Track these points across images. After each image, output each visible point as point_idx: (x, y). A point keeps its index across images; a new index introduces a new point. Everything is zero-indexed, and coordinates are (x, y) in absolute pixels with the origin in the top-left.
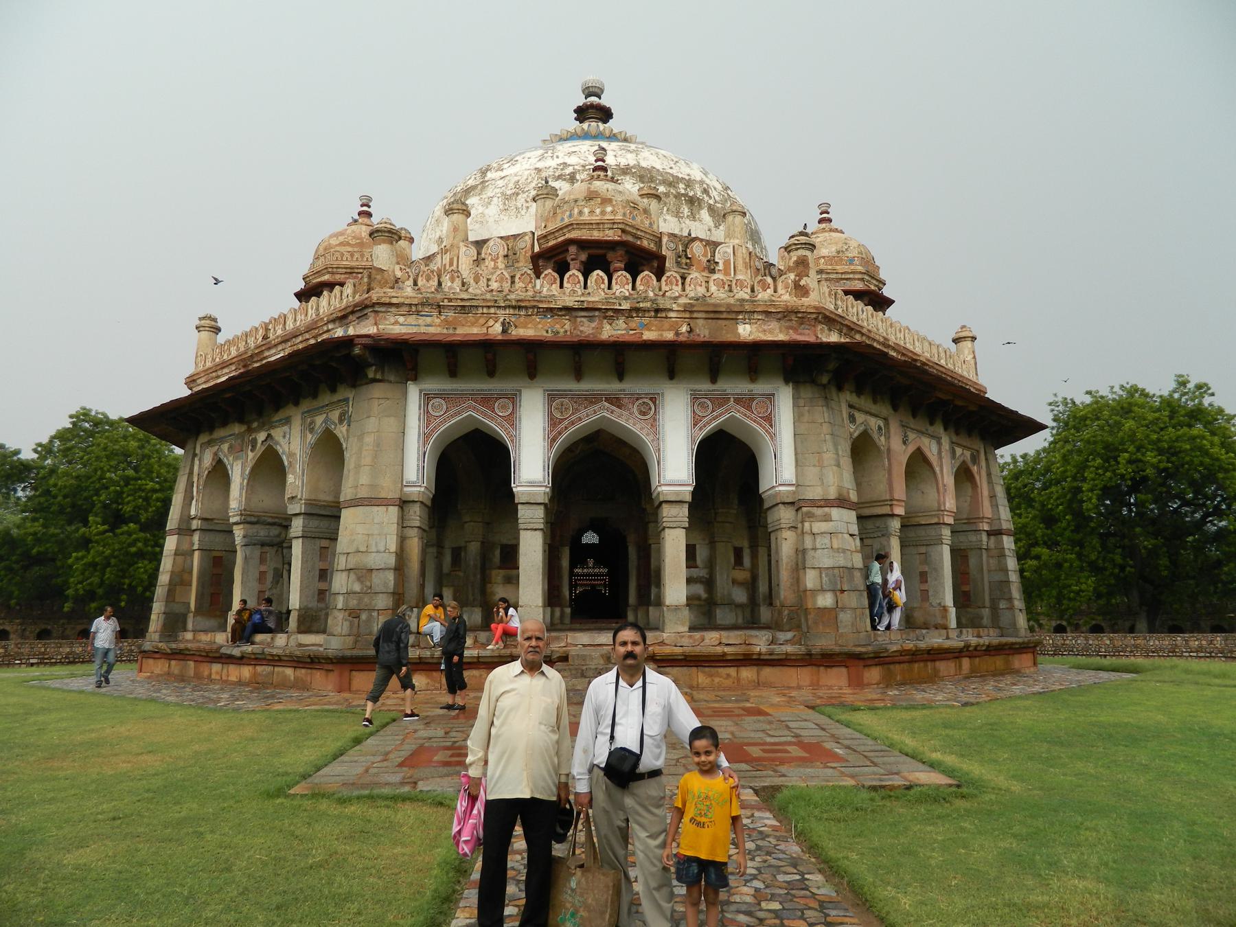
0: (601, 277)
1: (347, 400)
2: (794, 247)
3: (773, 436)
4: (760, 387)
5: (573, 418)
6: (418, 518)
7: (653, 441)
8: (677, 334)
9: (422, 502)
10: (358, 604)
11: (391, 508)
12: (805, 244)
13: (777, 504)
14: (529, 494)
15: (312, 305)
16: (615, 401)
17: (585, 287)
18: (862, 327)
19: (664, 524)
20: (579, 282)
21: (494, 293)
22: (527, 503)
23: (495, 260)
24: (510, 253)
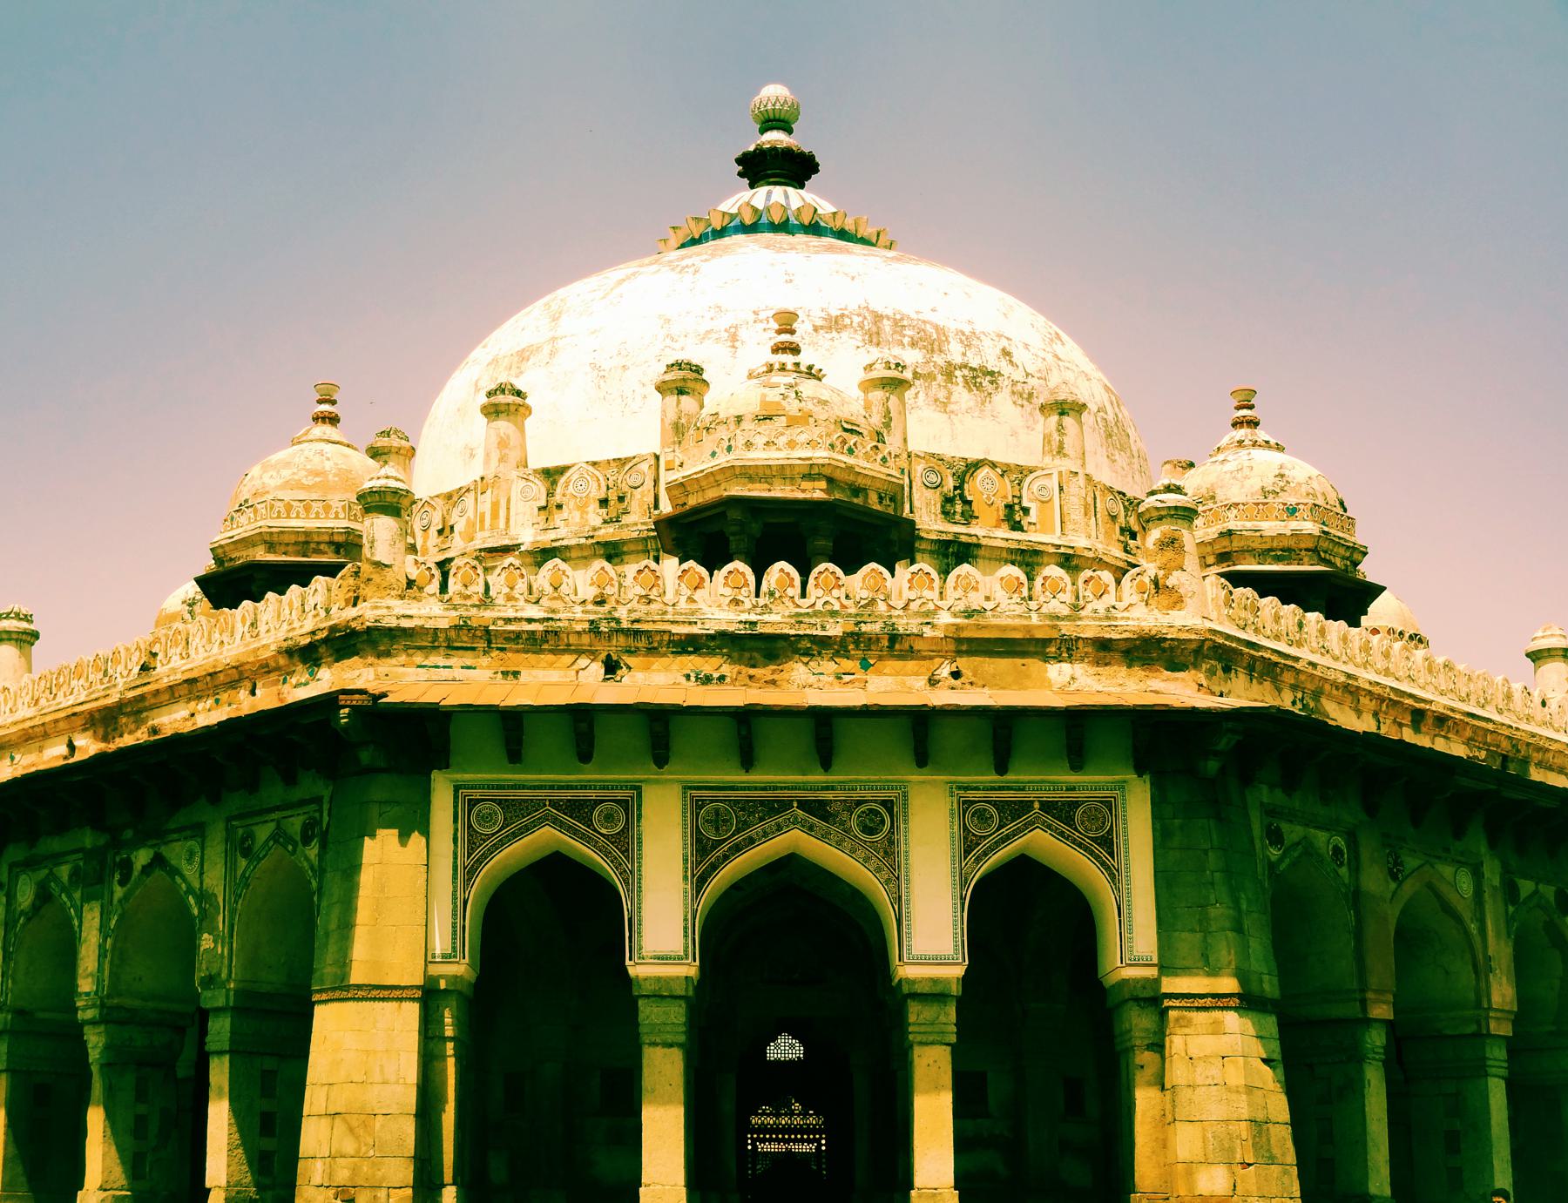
1: (318, 800)
2: (1155, 514)
3: (1113, 875)
4: (1088, 783)
5: (739, 838)
7: (888, 881)
8: (933, 682)
9: (460, 993)
10: (351, 1179)
11: (407, 1005)
12: (1176, 508)
15: (244, 616)
16: (818, 809)
18: (1297, 659)
22: (655, 996)
23: (582, 508)
24: (613, 497)
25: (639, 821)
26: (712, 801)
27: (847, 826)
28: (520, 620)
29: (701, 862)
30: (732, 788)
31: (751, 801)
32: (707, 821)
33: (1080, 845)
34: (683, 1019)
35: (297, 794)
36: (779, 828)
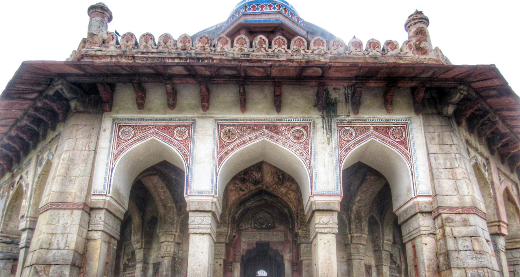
0: (263, 40)
5: (238, 142)
6: (103, 223)
9: (107, 210)
13: (416, 214)
14: (199, 202)
16: (274, 129)
17: (251, 46)
19: (317, 230)
20: (246, 43)
21: (179, 50)
22: (197, 211)
25: (194, 133)
26: (227, 126)
27: (288, 136)
28: (148, 52)
29: (221, 151)
30: (237, 120)
31: (244, 126)
32: (225, 134)
33: (392, 144)
34: (210, 222)
35: (56, 133)
36: (257, 137)
